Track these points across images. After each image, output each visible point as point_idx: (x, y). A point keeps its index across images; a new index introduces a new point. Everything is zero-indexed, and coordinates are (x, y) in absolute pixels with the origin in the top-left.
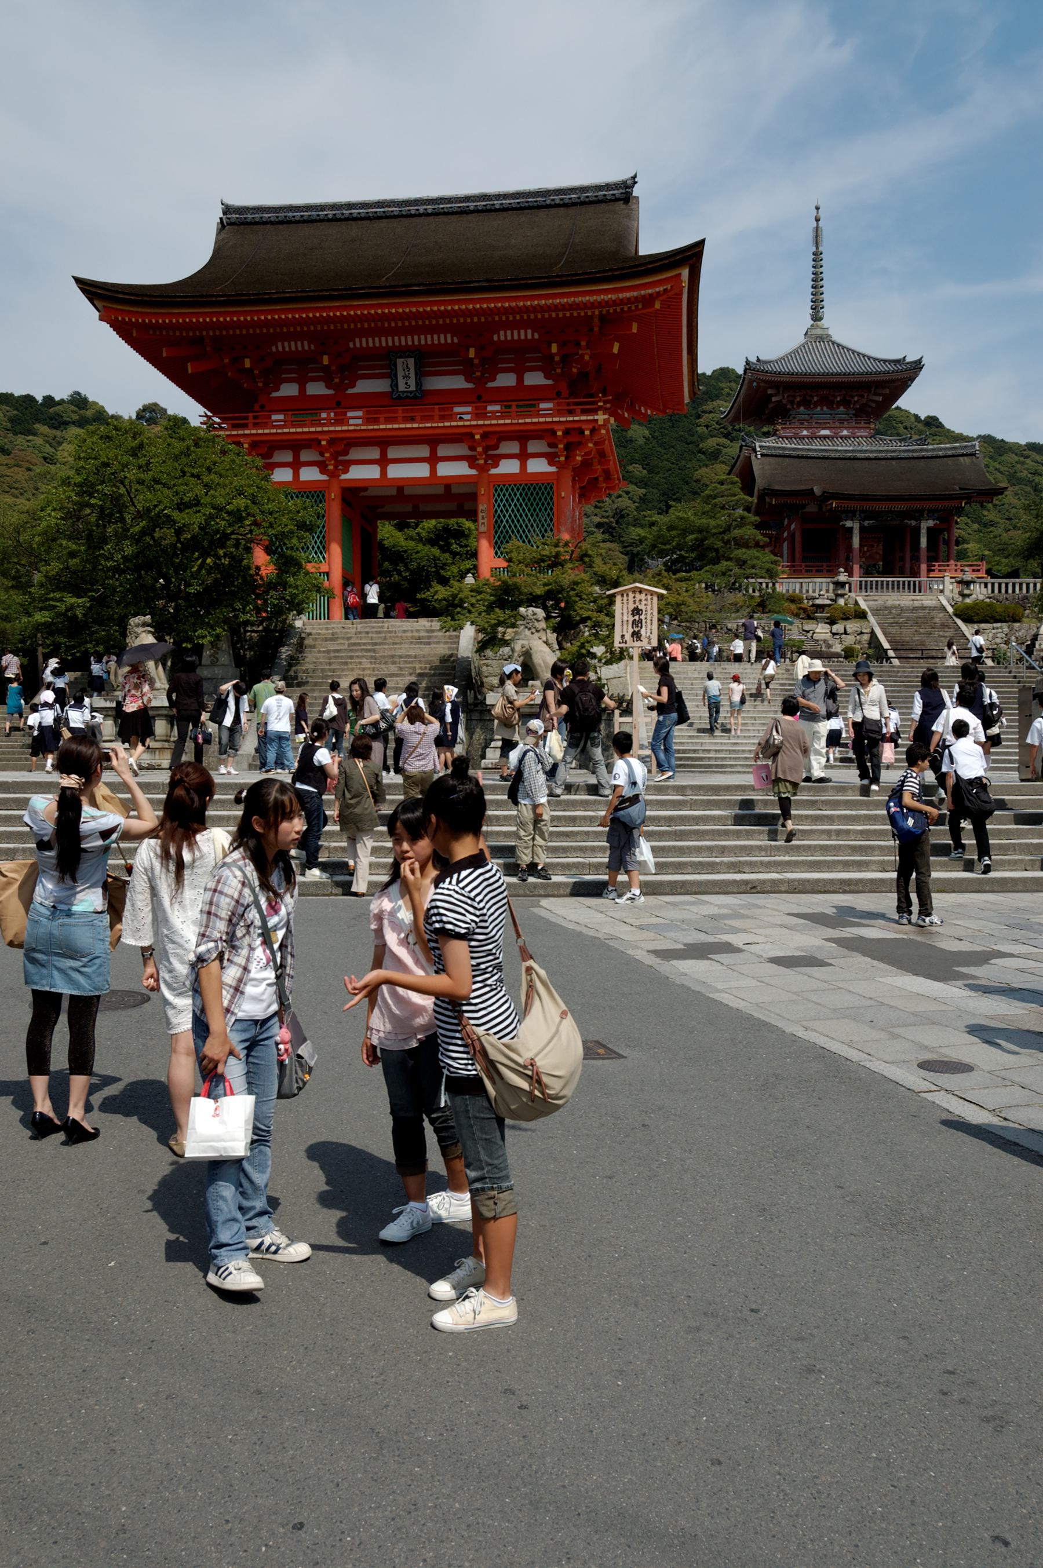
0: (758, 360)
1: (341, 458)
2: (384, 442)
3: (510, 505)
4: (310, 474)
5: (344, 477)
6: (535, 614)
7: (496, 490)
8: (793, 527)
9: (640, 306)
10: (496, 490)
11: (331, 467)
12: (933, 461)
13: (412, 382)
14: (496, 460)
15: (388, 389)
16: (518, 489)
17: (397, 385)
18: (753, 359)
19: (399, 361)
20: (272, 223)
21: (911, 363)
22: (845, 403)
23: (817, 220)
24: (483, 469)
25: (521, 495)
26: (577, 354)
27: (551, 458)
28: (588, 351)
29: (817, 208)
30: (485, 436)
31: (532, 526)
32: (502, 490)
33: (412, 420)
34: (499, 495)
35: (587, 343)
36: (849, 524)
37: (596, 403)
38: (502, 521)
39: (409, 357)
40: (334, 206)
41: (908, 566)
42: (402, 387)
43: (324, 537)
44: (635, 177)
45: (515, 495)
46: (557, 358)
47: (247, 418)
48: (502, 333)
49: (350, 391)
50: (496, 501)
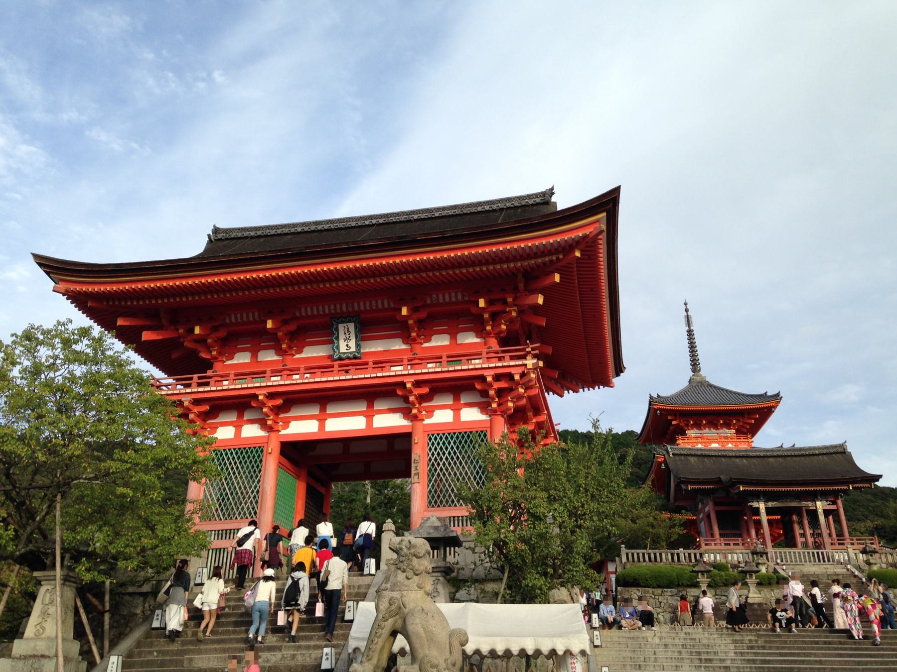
0: (658, 396)
1: (282, 415)
2: (323, 399)
3: (444, 454)
4: (252, 431)
5: (283, 432)
6: (410, 545)
7: (430, 439)
8: (707, 509)
9: (561, 257)
10: (430, 439)
11: (269, 422)
12: (811, 457)
13: (352, 344)
14: (430, 413)
15: (332, 353)
16: (452, 438)
17: (338, 347)
18: (656, 396)
19: (341, 327)
20: (252, 237)
21: (772, 396)
22: (728, 425)
23: (687, 311)
24: (415, 418)
25: (455, 442)
26: (505, 312)
27: (484, 407)
28: (515, 308)
29: (686, 304)
30: (418, 384)
31: (461, 463)
32: (436, 439)
33: (347, 372)
34: (433, 444)
35: (514, 300)
36: (755, 505)
37: (524, 350)
38: (436, 470)
39: (350, 321)
40: (303, 224)
41: (810, 540)
42: (343, 349)
43: (258, 492)
44: (552, 189)
45: (449, 443)
46: (486, 316)
47: (191, 379)
48: (434, 296)
49: (297, 356)
50: (430, 449)
